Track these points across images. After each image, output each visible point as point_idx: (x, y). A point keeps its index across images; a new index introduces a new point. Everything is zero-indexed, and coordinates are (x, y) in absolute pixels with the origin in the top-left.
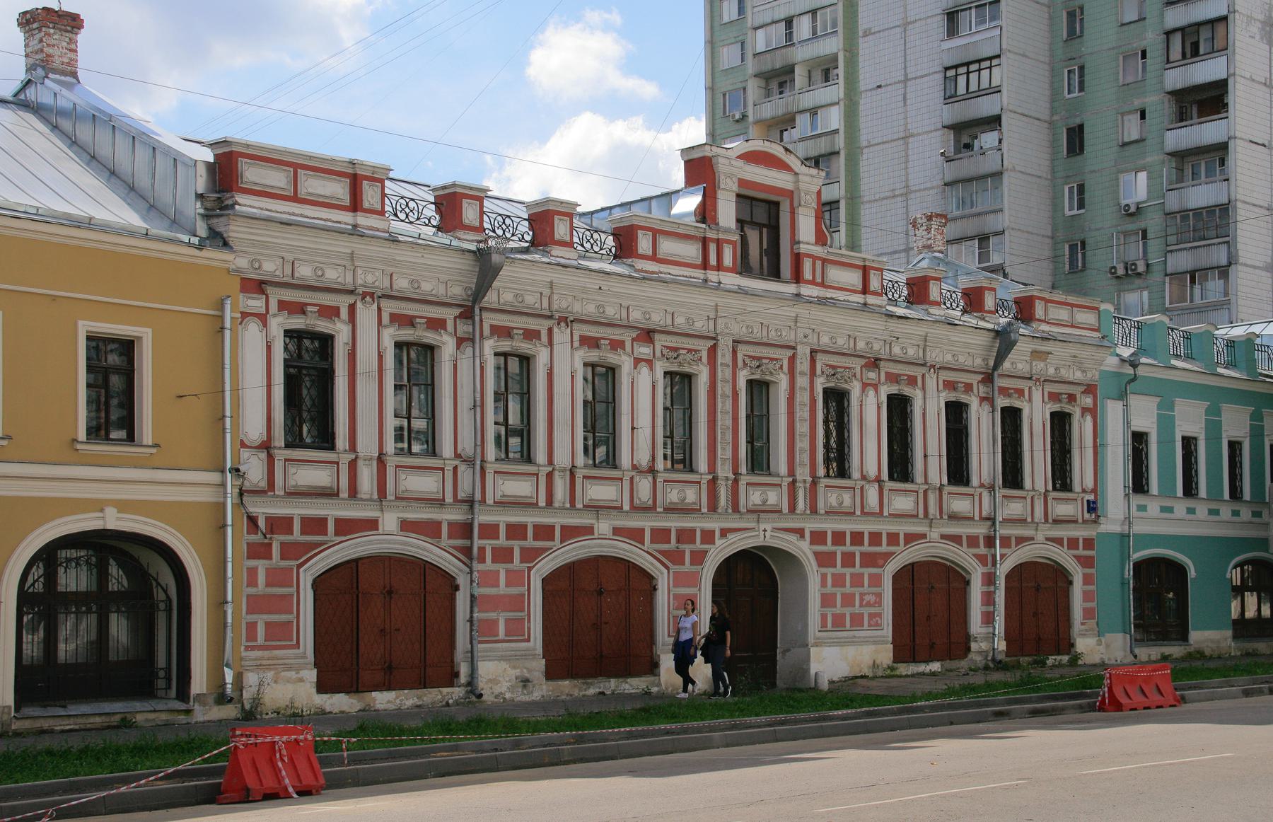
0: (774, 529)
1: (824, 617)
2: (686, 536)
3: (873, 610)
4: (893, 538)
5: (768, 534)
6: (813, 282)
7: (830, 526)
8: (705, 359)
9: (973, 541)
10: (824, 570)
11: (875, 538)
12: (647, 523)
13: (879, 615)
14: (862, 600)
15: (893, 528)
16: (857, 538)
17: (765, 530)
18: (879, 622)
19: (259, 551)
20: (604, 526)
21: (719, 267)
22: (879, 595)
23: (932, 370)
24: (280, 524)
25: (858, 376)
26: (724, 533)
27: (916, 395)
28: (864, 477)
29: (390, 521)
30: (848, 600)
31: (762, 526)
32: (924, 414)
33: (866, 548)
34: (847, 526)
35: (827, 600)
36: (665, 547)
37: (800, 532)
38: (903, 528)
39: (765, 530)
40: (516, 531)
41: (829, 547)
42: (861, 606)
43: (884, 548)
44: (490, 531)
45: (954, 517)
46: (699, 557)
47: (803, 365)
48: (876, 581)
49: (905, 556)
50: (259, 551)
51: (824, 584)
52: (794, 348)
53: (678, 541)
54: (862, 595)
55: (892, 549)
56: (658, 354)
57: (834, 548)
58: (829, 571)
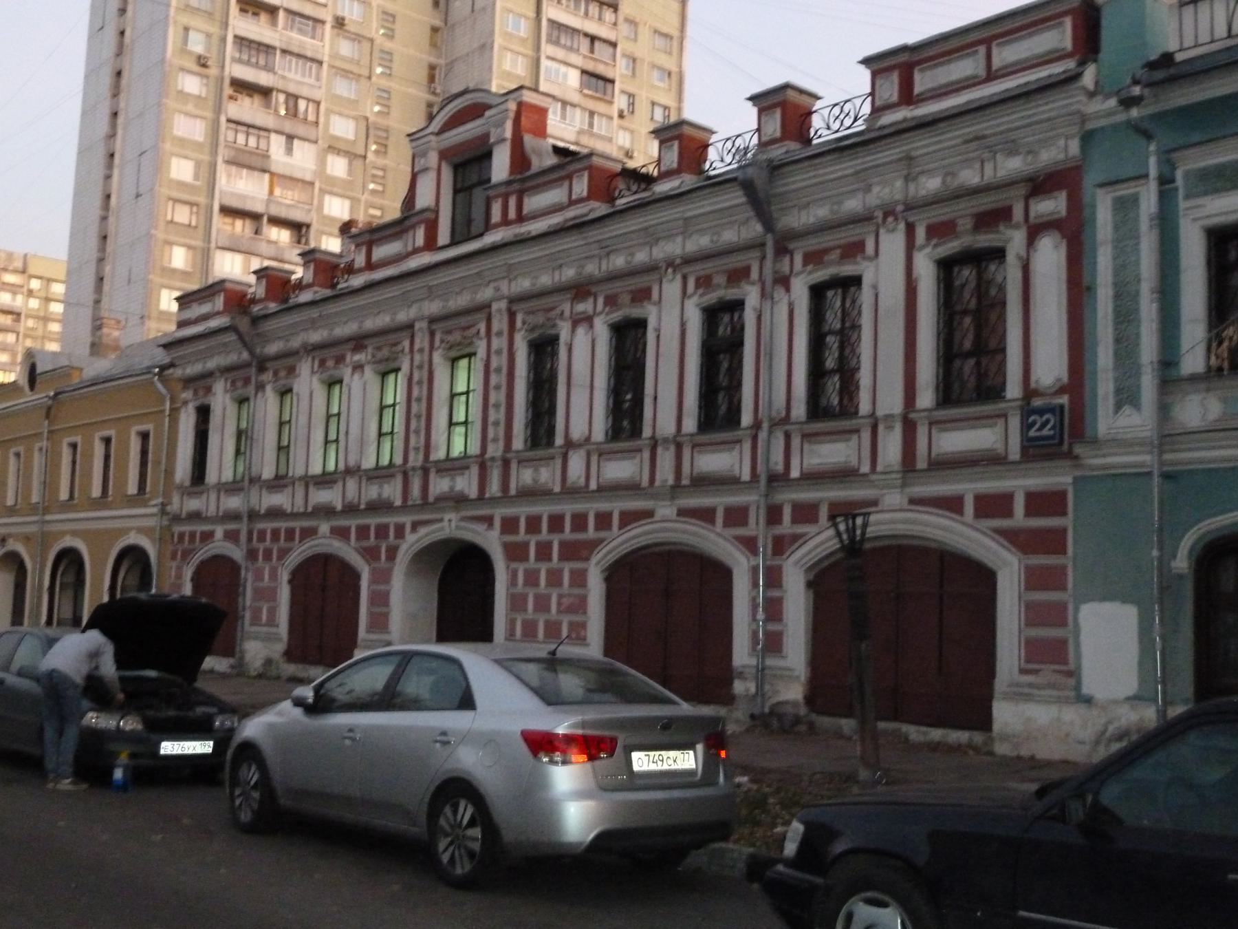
0: (463, 519)
1: (511, 624)
2: (382, 531)
3: (577, 618)
4: (604, 521)
5: (453, 524)
6: (505, 222)
7: (522, 511)
8: (407, 349)
9: (736, 516)
10: (514, 565)
11: (579, 522)
12: (353, 523)
13: (583, 626)
14: (559, 604)
15: (604, 506)
16: (556, 523)
17: (450, 521)
18: (583, 633)
19: (174, 557)
20: (324, 528)
21: (416, 251)
22: (583, 600)
23: (670, 270)
24: (182, 536)
25: (567, 313)
26: (415, 526)
27: (650, 312)
28: (570, 445)
29: (219, 532)
30: (542, 604)
31: (447, 517)
32: (658, 337)
33: (568, 534)
34: (544, 510)
35: (516, 603)
36: (365, 544)
37: (489, 520)
38: (616, 507)
39: (450, 521)
40: (275, 534)
41: (522, 535)
42: (559, 611)
43: (591, 533)
44: (262, 536)
45: (703, 482)
46: (392, 553)
47: (500, 323)
48: (579, 579)
49: (619, 542)
50: (174, 557)
51: (513, 581)
52: (489, 306)
53: (377, 537)
54: (560, 597)
55: (602, 534)
56: (369, 357)
57: (528, 537)
58: (521, 568)
